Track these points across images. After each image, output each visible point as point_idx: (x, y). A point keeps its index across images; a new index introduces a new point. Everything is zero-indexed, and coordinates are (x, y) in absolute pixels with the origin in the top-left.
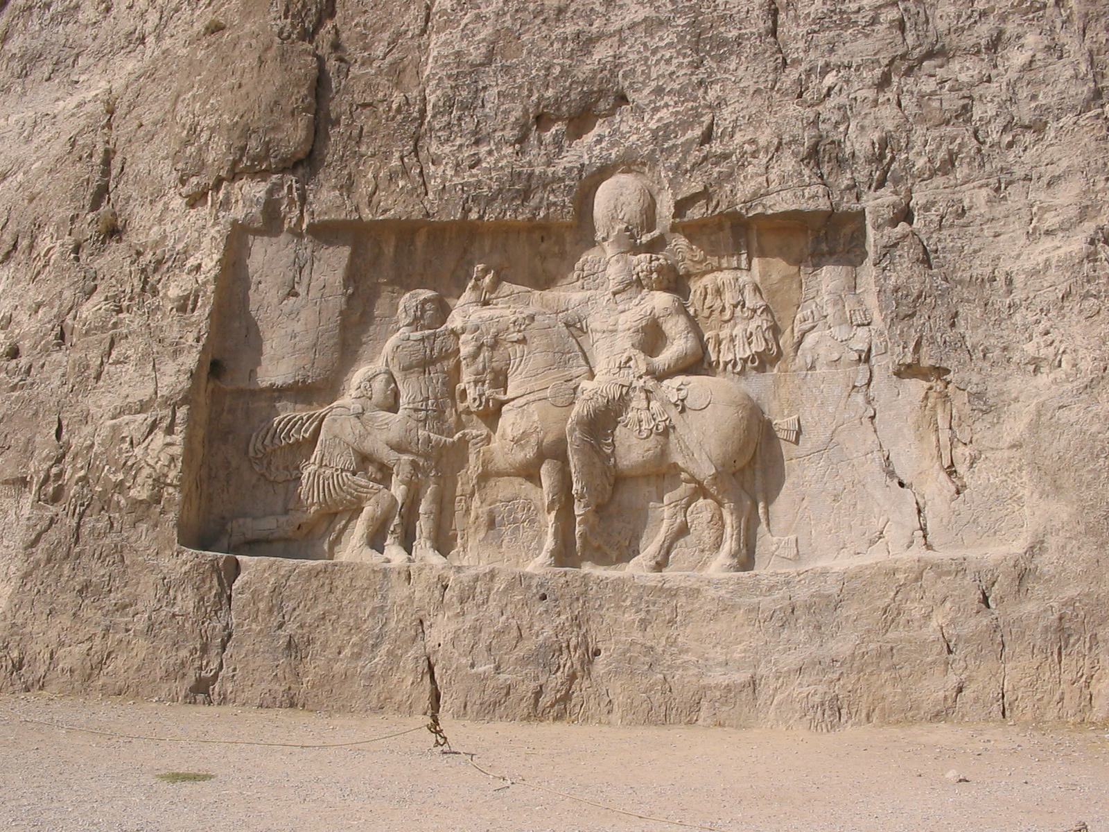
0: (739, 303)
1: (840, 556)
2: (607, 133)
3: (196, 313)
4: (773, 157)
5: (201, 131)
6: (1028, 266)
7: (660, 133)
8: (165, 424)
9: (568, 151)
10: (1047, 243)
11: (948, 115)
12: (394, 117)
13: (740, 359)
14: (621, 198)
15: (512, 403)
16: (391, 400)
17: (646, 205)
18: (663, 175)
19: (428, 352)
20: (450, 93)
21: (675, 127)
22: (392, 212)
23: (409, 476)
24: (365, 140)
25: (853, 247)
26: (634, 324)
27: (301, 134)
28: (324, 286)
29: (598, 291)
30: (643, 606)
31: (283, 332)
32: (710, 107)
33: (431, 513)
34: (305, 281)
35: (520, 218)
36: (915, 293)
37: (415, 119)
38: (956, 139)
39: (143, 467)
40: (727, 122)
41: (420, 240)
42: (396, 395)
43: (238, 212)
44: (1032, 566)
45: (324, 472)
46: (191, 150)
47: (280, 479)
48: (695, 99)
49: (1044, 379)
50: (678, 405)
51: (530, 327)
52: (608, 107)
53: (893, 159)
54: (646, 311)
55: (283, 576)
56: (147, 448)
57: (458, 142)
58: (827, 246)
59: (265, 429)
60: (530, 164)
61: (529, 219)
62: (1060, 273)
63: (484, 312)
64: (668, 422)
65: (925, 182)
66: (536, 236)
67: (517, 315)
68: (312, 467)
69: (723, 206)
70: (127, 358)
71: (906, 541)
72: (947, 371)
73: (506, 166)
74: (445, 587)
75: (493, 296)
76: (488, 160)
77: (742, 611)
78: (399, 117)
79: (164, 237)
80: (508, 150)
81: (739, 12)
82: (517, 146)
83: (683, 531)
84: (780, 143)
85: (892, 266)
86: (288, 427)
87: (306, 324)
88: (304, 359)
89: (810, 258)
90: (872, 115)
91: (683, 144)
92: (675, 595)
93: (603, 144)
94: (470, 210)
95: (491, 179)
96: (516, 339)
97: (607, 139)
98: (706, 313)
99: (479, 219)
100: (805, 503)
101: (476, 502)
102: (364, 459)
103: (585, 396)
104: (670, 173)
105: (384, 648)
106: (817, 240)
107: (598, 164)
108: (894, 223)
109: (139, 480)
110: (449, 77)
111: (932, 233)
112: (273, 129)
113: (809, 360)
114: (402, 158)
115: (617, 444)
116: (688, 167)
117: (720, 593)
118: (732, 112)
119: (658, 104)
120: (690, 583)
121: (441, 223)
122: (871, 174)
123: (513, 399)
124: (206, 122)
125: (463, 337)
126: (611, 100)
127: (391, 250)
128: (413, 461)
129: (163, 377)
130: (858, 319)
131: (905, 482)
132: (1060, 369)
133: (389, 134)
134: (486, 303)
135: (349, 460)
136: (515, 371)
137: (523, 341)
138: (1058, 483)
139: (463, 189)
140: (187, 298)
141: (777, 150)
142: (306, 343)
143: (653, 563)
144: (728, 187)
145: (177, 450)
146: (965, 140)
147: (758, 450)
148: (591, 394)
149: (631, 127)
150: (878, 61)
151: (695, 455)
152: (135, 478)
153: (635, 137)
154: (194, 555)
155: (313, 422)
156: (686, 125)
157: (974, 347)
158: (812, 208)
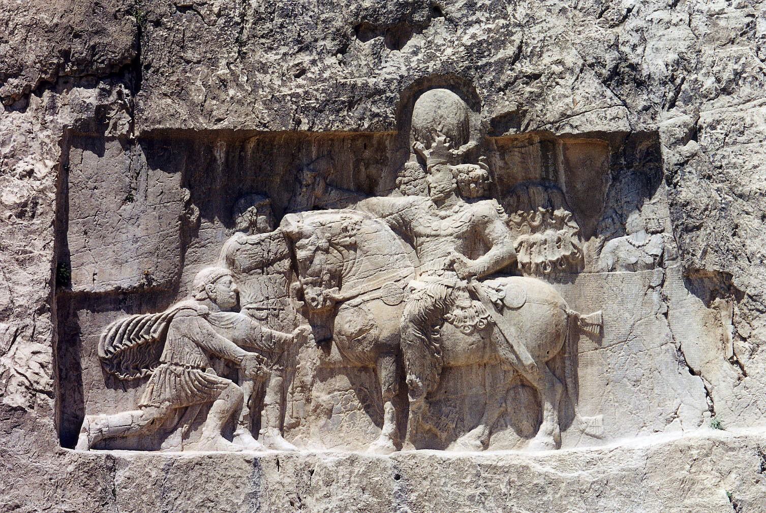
1: (640, 434)
3: (34, 221)
4: (577, 78)
7: (475, 50)
8: (29, 332)
9: (386, 62)
11: (733, 35)
12: (215, 21)
13: (550, 261)
14: (439, 112)
15: (348, 302)
17: (462, 119)
18: (478, 91)
19: (265, 255)
21: (488, 45)
22: (226, 123)
23: (256, 370)
25: (647, 162)
26: (457, 230)
27: (126, 40)
28: (162, 192)
29: (420, 197)
30: (481, 482)
31: (124, 237)
32: (520, 25)
33: (277, 403)
35: (346, 129)
36: (703, 207)
37: (238, 24)
38: (740, 59)
39: (13, 376)
40: (536, 42)
42: (237, 293)
43: (65, 118)
45: (175, 370)
50: (495, 304)
51: (360, 231)
53: (684, 79)
54: (467, 218)
55: (163, 470)
56: (13, 357)
57: (283, 50)
58: (625, 160)
59: (113, 330)
60: (352, 74)
61: (355, 130)
63: (316, 216)
64: (489, 318)
65: (712, 101)
66: (359, 143)
68: (162, 365)
71: (697, 420)
72: (730, 276)
73: (331, 77)
74: (312, 472)
76: (312, 70)
77: (564, 484)
78: (221, 21)
80: (330, 60)
82: (340, 56)
84: (584, 65)
86: (136, 329)
87: (147, 229)
88: (147, 262)
89: (610, 171)
90: (666, 37)
91: (496, 63)
92: (507, 472)
93: (420, 56)
94: (299, 122)
95: (317, 90)
96: (348, 243)
97: (423, 50)
99: (309, 130)
102: (214, 356)
103: (416, 295)
104: (485, 91)
106: (616, 156)
107: (416, 77)
108: (684, 141)
109: (11, 388)
111: (717, 150)
112: (97, 33)
113: (610, 263)
114: (228, 64)
115: (444, 338)
116: (501, 84)
117: (545, 470)
118: (539, 32)
119: (470, 19)
120: (519, 461)
122: (664, 96)
123: (349, 299)
126: (426, 12)
127: (222, 155)
128: (258, 357)
129: (16, 287)
130: (653, 226)
131: (695, 370)
133: (213, 39)
134: (316, 208)
135: (196, 357)
136: (348, 273)
137: (353, 247)
139: (291, 100)
140: (25, 205)
141: (581, 71)
142: (149, 247)
143: (478, 443)
144: (539, 106)
145: (47, 356)
146: (749, 60)
147: (567, 341)
148: (420, 294)
149: (445, 39)
151: (515, 348)
153: (449, 51)
154: (77, 456)
155: (160, 324)
156: (500, 44)
158: (613, 129)
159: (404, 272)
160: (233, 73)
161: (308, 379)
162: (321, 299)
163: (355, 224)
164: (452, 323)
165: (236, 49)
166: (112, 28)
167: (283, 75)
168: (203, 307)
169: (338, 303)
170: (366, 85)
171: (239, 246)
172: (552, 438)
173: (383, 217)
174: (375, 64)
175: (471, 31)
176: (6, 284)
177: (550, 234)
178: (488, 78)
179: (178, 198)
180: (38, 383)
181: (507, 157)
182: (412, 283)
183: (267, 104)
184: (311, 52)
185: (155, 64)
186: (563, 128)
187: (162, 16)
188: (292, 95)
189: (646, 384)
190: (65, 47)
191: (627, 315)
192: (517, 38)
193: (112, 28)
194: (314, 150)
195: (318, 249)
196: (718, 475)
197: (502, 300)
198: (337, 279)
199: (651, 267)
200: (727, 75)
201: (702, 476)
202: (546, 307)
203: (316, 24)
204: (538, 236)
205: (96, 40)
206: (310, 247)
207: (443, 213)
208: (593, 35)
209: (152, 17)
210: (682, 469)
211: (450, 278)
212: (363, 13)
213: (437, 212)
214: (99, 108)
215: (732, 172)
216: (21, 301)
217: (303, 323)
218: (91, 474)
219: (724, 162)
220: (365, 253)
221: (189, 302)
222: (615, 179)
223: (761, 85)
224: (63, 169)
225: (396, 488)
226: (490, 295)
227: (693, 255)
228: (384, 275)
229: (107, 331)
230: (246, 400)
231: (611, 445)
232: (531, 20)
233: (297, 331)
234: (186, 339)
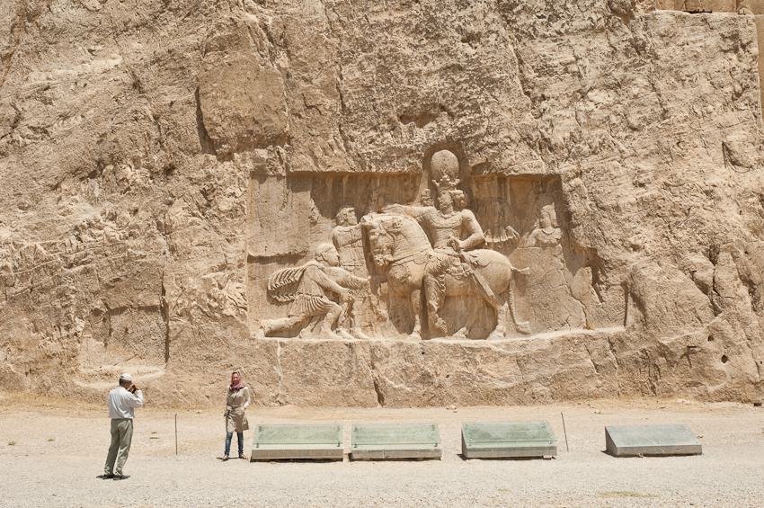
6: (633, 200)
10: (642, 190)
41: (345, 181)
43: (250, 166)
46: (219, 129)
48: (480, 112)
49: (636, 254)
50: (474, 264)
57: (363, 129)
66: (402, 179)
69: (493, 171)
72: (596, 250)
80: (387, 135)
81: (500, 63)
94: (370, 168)
102: (327, 290)
105: (352, 381)
110: (354, 93)
113: (534, 242)
125: (372, 231)
134: (379, 212)
137: (399, 233)
150: (567, 94)
153: (450, 130)
156: (476, 127)
159: (426, 247)
160: (336, 141)
162: (382, 260)
168: (321, 265)
170: (405, 148)
173: (415, 217)
175: (461, 120)
178: (470, 145)
182: (431, 252)
186: (509, 171)
188: (367, 153)
189: (552, 306)
190: (251, 128)
191: (542, 270)
192: (486, 124)
193: (274, 118)
198: (392, 250)
200: (595, 144)
202: (500, 265)
207: (446, 216)
208: (525, 122)
211: (450, 251)
215: (597, 196)
218: (268, 350)
219: (594, 190)
222: (537, 198)
223: (613, 150)
225: (423, 359)
230: (343, 312)
231: (533, 337)
232: (494, 114)
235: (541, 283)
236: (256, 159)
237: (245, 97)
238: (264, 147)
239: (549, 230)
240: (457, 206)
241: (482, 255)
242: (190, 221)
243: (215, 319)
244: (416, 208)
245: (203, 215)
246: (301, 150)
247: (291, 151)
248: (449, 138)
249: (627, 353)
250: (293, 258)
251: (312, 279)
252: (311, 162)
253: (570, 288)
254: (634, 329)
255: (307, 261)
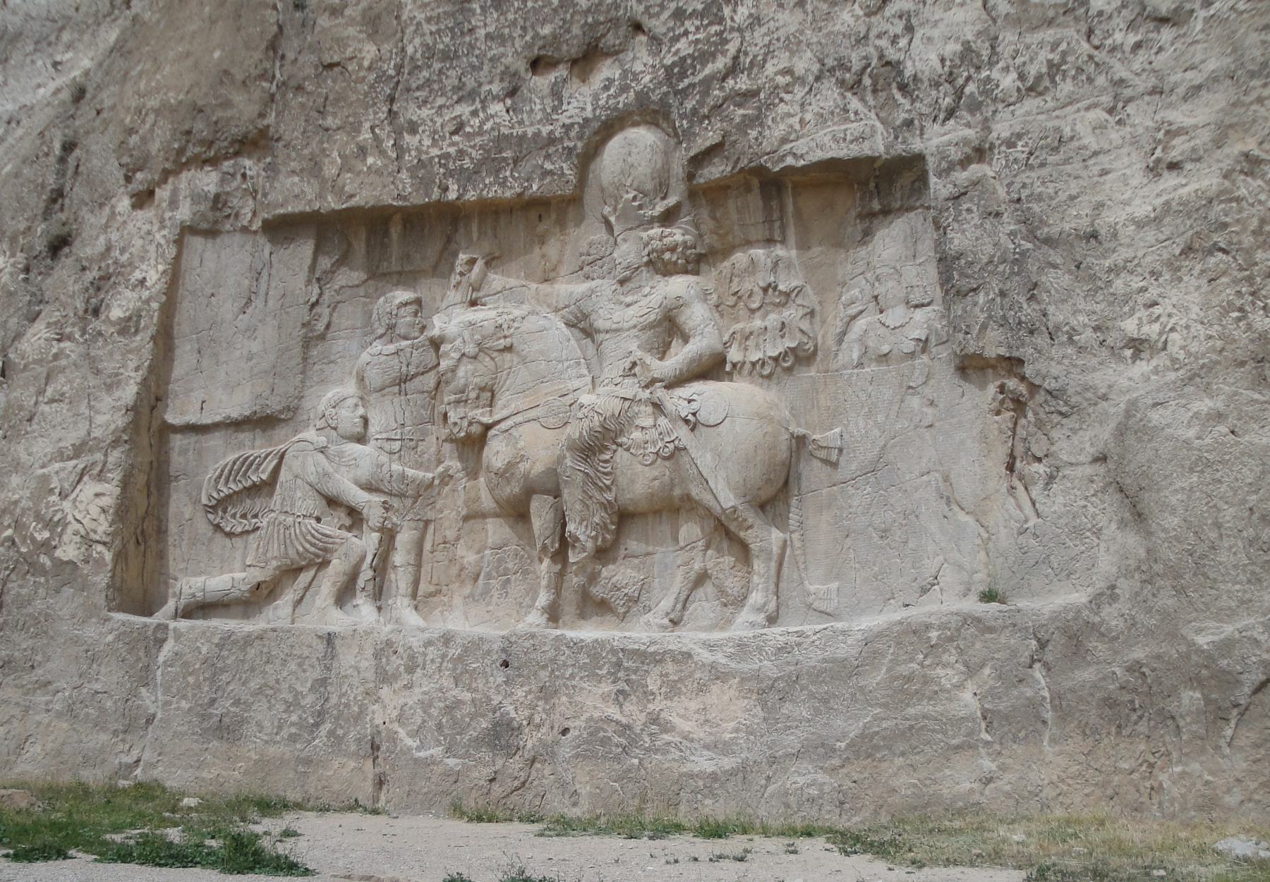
0: (769, 285)
2: (617, 76)
5: (146, 114)
8: (96, 471)
12: (364, 78)
13: (770, 357)
16: (360, 429)
17: (659, 165)
19: (404, 369)
20: (429, 40)
24: (330, 109)
26: (641, 320)
29: (606, 281)
31: (238, 353)
34: (263, 286)
35: (508, 194)
41: (395, 232)
42: (366, 421)
43: (184, 213)
44: (1097, 619)
46: (134, 140)
47: (239, 530)
50: (687, 421)
52: (617, 42)
57: (440, 101)
61: (520, 195)
62: (1179, 221)
67: (505, 316)
69: (744, 162)
70: (63, 395)
71: (962, 588)
73: (493, 129)
75: (481, 294)
78: (372, 77)
79: (109, 249)
80: (496, 108)
82: (509, 102)
83: (702, 579)
85: (956, 225)
93: (612, 91)
94: (446, 189)
98: (731, 301)
100: (849, 542)
101: (461, 550)
102: (332, 502)
104: (685, 122)
110: (429, 20)
113: (855, 355)
114: (372, 128)
115: (618, 472)
121: (414, 206)
123: (499, 422)
124: (153, 103)
126: (622, 31)
128: (384, 502)
132: (1163, 353)
133: (358, 100)
134: (473, 303)
137: (509, 349)
138: (1138, 507)
140: (130, 318)
152: (60, 536)
155: (271, 461)
157: (1058, 328)
159: (577, 383)
160: (376, 138)
161: (450, 534)
162: (465, 423)
163: (513, 321)
164: (628, 450)
165: (385, 109)
166: (238, 98)
167: (435, 132)
169: (488, 427)
170: (537, 134)
171: (368, 359)
172: (763, 615)
173: (557, 310)
174: (555, 109)
176: (87, 412)
177: (773, 319)
179: (301, 301)
180: (95, 532)
181: (718, 215)
183: (412, 171)
184: (474, 101)
185: (287, 137)
187: (304, 79)
188: (440, 157)
190: (186, 127)
191: (876, 432)
193: (238, 98)
194: (475, 227)
195: (463, 355)
196: (963, 669)
197: (694, 414)
199: (912, 355)
201: (940, 671)
203: (482, 63)
204: (758, 323)
205: (220, 113)
206: (453, 355)
207: (629, 299)
209: (293, 83)
210: (912, 660)
211: (630, 388)
212: (541, 43)
213: (622, 298)
214: (217, 197)
216: (97, 433)
217: (451, 458)
220: (524, 361)
221: (310, 434)
224: (174, 276)
226: (680, 408)
227: (967, 333)
228: (547, 388)
229: (211, 474)
233: (441, 469)
234: (299, 481)
235: (872, 469)
236: (196, 198)
237: (190, 62)
238: (213, 162)
239: (895, 316)
240: (660, 265)
241: (707, 394)
242: (54, 351)
243: (44, 572)
244: (568, 289)
245: (84, 332)
246: (294, 165)
247: (272, 170)
248: (642, 97)
249: (1087, 675)
250: (262, 422)
251: (297, 477)
252: (310, 190)
253: (946, 479)
254: (1114, 598)
255: (296, 432)
